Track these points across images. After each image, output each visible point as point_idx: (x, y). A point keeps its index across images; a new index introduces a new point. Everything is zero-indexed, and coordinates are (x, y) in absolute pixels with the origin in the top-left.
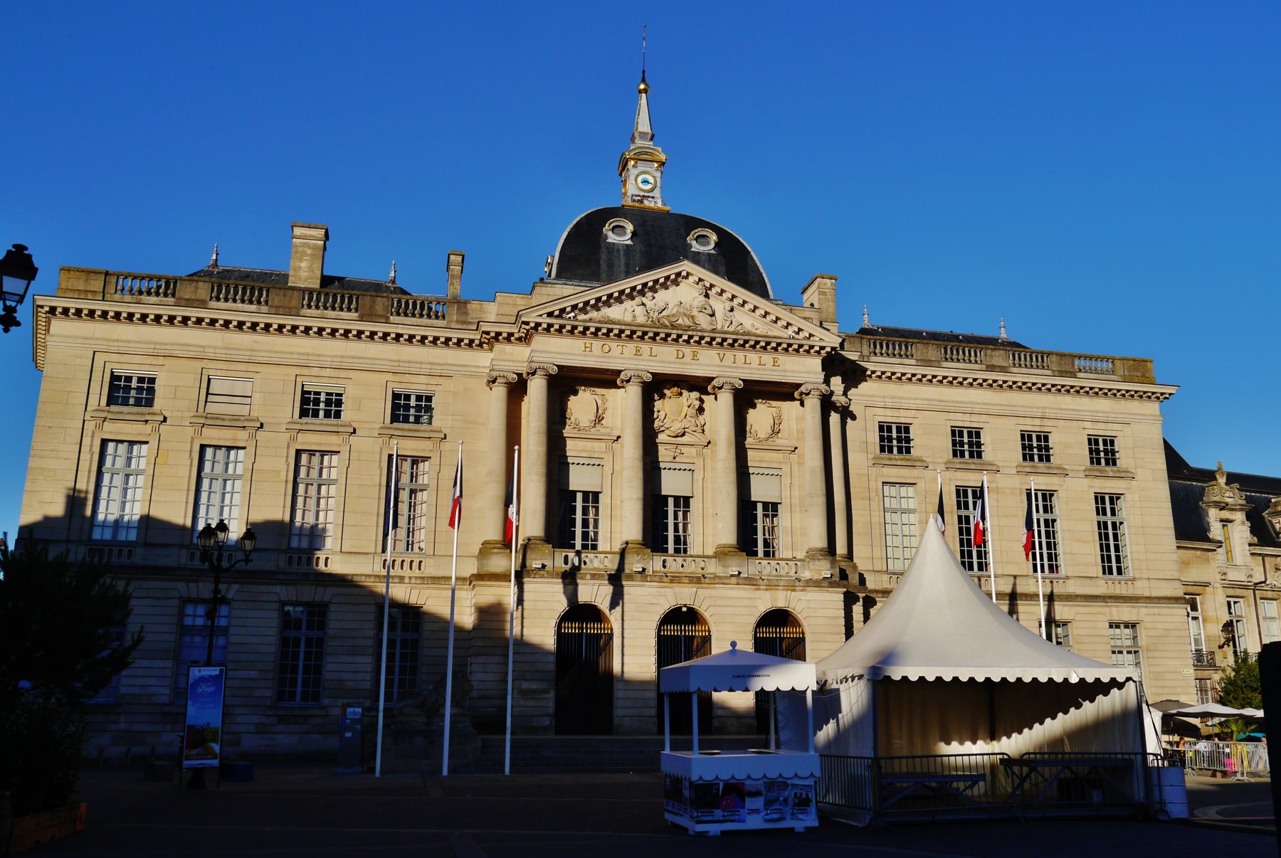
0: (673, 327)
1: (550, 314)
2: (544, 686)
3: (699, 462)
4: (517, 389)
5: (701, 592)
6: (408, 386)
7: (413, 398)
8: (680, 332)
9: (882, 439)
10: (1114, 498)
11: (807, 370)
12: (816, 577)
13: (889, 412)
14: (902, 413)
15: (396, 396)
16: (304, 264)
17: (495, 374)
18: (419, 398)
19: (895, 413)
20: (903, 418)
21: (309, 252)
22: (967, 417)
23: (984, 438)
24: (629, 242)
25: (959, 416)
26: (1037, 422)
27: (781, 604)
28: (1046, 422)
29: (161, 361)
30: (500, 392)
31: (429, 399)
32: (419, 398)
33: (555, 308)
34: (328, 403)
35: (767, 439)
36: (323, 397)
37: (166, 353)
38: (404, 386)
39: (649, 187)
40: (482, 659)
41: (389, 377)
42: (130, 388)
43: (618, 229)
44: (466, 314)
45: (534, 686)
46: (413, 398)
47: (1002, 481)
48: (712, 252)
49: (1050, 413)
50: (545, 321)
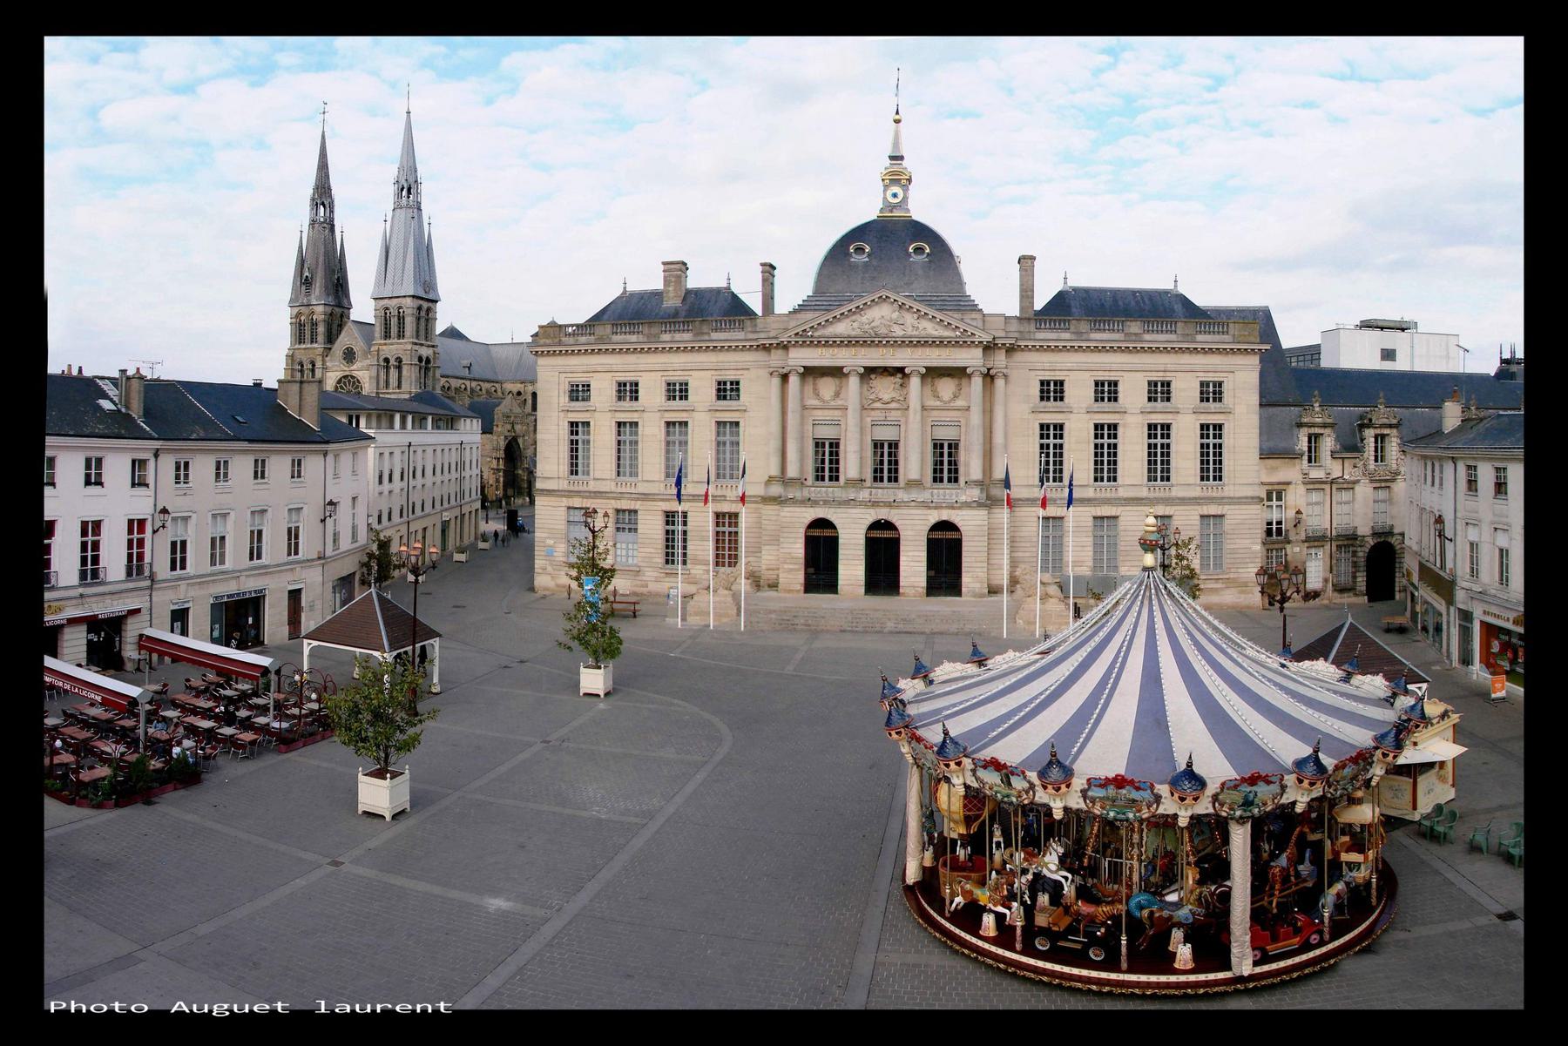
0: (877, 335)
1: (797, 334)
2: (797, 567)
3: (903, 420)
4: (785, 378)
5: (892, 511)
6: (725, 377)
7: (728, 384)
8: (880, 339)
9: (1042, 391)
10: (1219, 427)
11: (971, 358)
12: (969, 500)
13: (1047, 373)
14: (1058, 373)
15: (719, 383)
16: (670, 289)
17: (772, 370)
18: (732, 383)
19: (1052, 373)
20: (1058, 376)
21: (673, 280)
22: (1107, 374)
23: (1120, 388)
24: (867, 259)
25: (1100, 373)
26: (1161, 374)
27: (944, 518)
28: (1168, 374)
29: (591, 375)
30: (776, 381)
31: (738, 383)
32: (732, 383)
33: (799, 330)
34: (681, 391)
35: (950, 402)
36: (677, 387)
37: (593, 369)
38: (722, 377)
39: (896, 200)
40: (767, 547)
41: (713, 372)
42: (578, 390)
43: (860, 250)
44: (756, 325)
45: (791, 566)
46: (728, 384)
47: (1130, 419)
48: (926, 260)
49: (1170, 367)
50: (793, 339)
